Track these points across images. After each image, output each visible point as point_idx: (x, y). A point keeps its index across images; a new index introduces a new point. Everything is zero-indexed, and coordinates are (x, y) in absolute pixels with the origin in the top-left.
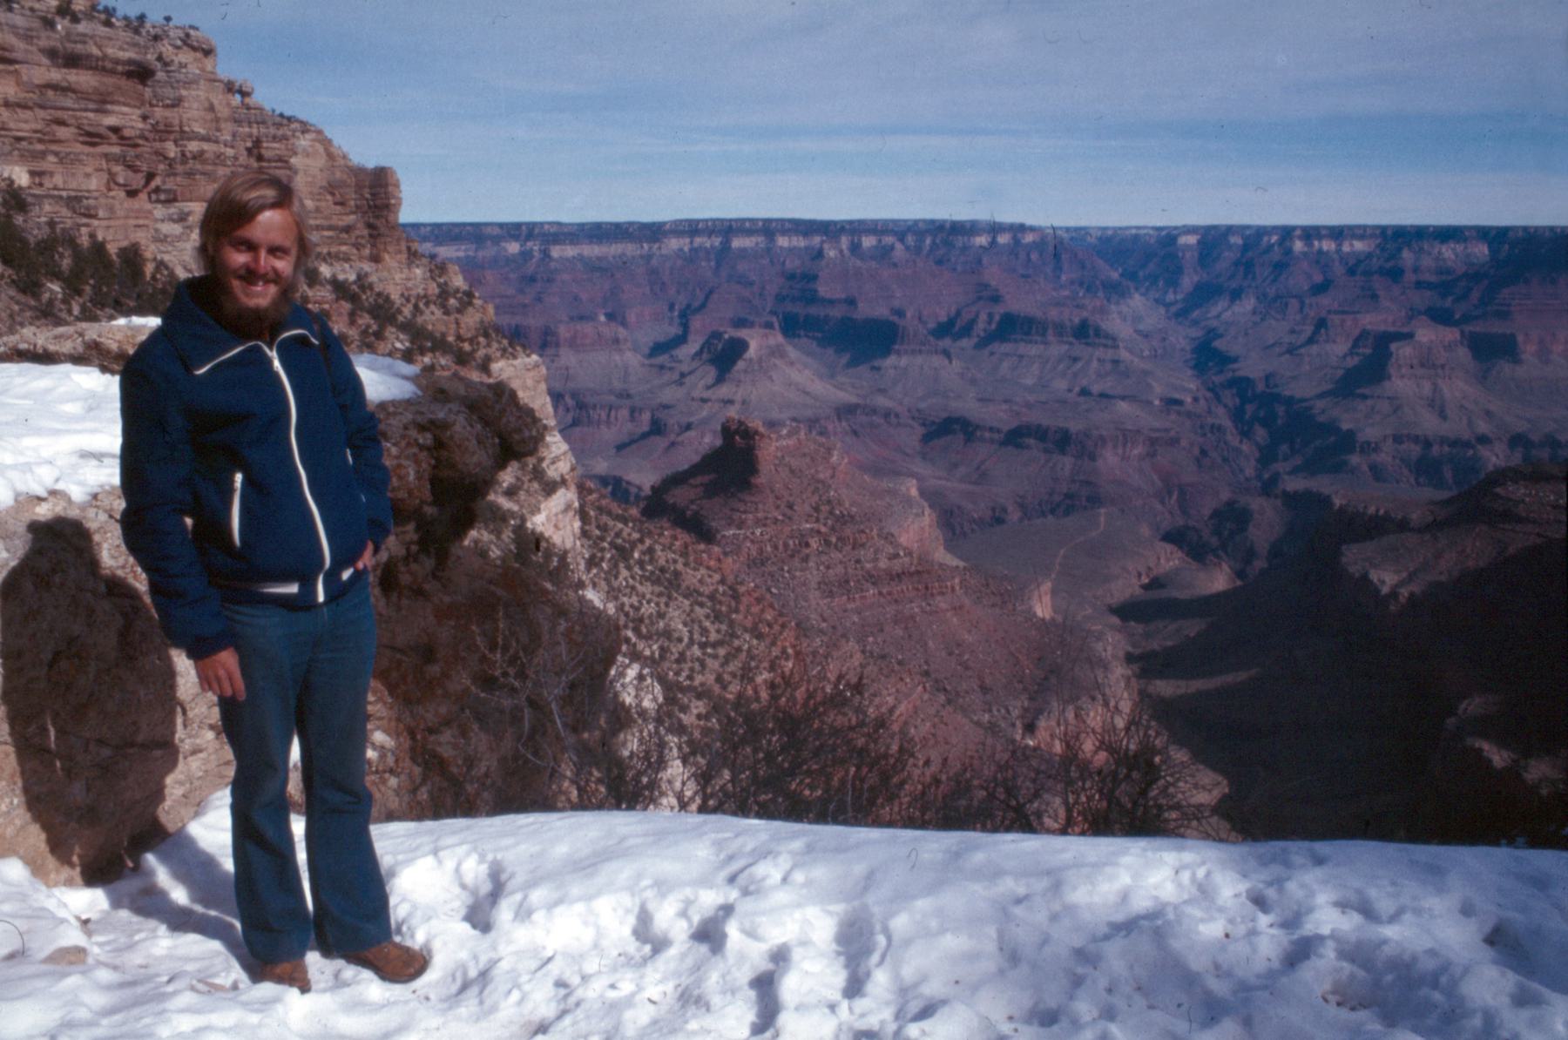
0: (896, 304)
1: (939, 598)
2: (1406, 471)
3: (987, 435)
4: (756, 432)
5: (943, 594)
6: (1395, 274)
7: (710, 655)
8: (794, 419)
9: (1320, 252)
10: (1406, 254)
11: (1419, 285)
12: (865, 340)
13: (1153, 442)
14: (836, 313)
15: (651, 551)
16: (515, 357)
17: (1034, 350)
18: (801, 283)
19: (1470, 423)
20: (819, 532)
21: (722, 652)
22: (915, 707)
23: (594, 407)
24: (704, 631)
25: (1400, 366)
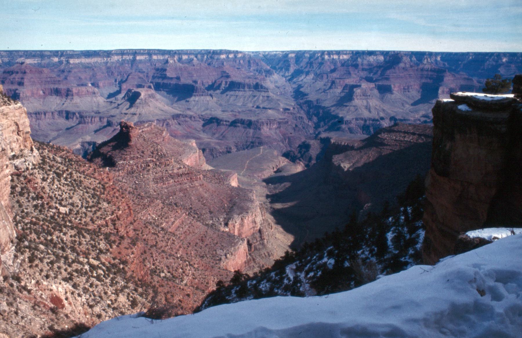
0: (194, 78)
1: (195, 182)
2: (359, 130)
3: (225, 123)
4: (130, 127)
5: (196, 180)
6: (356, 66)
7: (89, 211)
8: (158, 120)
9: (333, 59)
10: (359, 59)
11: (363, 70)
12: (182, 91)
13: (279, 123)
14: (174, 82)
15: (71, 174)
16: (10, 105)
17: (241, 93)
18: (161, 72)
19: (378, 114)
20: (153, 161)
21: (94, 209)
22: (182, 221)
23: (86, 117)
24: (88, 202)
25: (357, 96)
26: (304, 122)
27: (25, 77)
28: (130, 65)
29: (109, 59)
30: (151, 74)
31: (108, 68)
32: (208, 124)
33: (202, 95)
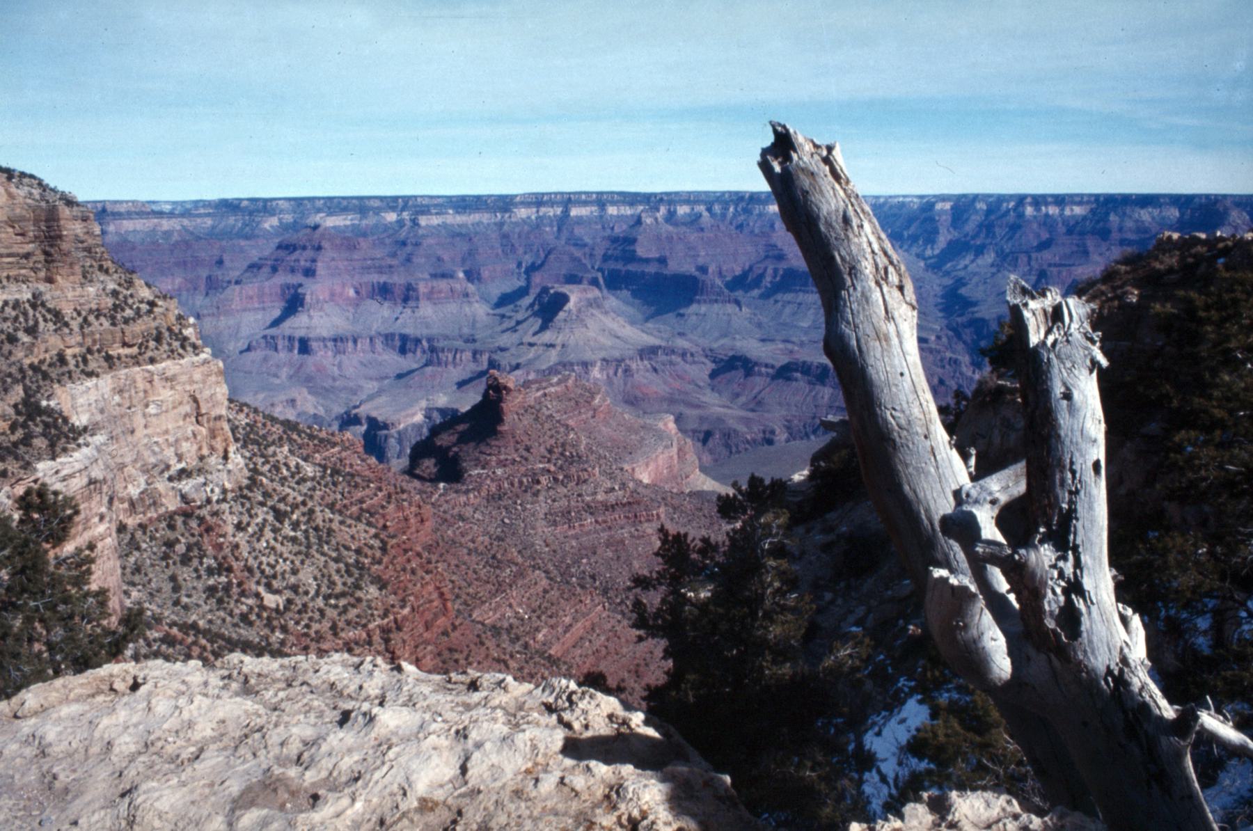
0: (701, 261)
1: (646, 525)
3: (763, 369)
4: (505, 388)
5: (648, 521)
6: (1104, 234)
7: (331, 606)
8: (604, 360)
9: (1047, 215)
14: (651, 269)
15: (311, 512)
16: (181, 356)
18: (623, 245)
20: (549, 471)
21: (342, 602)
22: (593, 624)
23: (443, 351)
24: (332, 584)
26: (961, 373)
27: (320, 258)
28: (555, 229)
29: (507, 215)
30: (599, 252)
31: (505, 236)
32: (724, 372)
33: (716, 301)
